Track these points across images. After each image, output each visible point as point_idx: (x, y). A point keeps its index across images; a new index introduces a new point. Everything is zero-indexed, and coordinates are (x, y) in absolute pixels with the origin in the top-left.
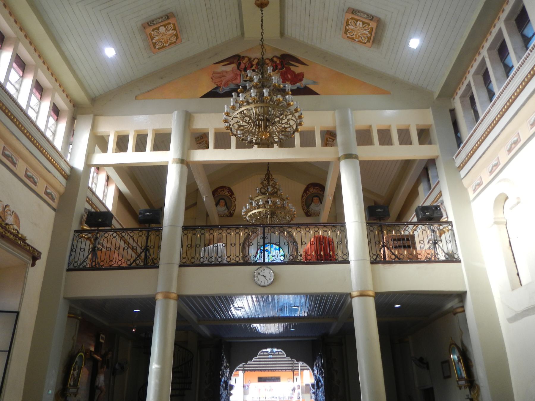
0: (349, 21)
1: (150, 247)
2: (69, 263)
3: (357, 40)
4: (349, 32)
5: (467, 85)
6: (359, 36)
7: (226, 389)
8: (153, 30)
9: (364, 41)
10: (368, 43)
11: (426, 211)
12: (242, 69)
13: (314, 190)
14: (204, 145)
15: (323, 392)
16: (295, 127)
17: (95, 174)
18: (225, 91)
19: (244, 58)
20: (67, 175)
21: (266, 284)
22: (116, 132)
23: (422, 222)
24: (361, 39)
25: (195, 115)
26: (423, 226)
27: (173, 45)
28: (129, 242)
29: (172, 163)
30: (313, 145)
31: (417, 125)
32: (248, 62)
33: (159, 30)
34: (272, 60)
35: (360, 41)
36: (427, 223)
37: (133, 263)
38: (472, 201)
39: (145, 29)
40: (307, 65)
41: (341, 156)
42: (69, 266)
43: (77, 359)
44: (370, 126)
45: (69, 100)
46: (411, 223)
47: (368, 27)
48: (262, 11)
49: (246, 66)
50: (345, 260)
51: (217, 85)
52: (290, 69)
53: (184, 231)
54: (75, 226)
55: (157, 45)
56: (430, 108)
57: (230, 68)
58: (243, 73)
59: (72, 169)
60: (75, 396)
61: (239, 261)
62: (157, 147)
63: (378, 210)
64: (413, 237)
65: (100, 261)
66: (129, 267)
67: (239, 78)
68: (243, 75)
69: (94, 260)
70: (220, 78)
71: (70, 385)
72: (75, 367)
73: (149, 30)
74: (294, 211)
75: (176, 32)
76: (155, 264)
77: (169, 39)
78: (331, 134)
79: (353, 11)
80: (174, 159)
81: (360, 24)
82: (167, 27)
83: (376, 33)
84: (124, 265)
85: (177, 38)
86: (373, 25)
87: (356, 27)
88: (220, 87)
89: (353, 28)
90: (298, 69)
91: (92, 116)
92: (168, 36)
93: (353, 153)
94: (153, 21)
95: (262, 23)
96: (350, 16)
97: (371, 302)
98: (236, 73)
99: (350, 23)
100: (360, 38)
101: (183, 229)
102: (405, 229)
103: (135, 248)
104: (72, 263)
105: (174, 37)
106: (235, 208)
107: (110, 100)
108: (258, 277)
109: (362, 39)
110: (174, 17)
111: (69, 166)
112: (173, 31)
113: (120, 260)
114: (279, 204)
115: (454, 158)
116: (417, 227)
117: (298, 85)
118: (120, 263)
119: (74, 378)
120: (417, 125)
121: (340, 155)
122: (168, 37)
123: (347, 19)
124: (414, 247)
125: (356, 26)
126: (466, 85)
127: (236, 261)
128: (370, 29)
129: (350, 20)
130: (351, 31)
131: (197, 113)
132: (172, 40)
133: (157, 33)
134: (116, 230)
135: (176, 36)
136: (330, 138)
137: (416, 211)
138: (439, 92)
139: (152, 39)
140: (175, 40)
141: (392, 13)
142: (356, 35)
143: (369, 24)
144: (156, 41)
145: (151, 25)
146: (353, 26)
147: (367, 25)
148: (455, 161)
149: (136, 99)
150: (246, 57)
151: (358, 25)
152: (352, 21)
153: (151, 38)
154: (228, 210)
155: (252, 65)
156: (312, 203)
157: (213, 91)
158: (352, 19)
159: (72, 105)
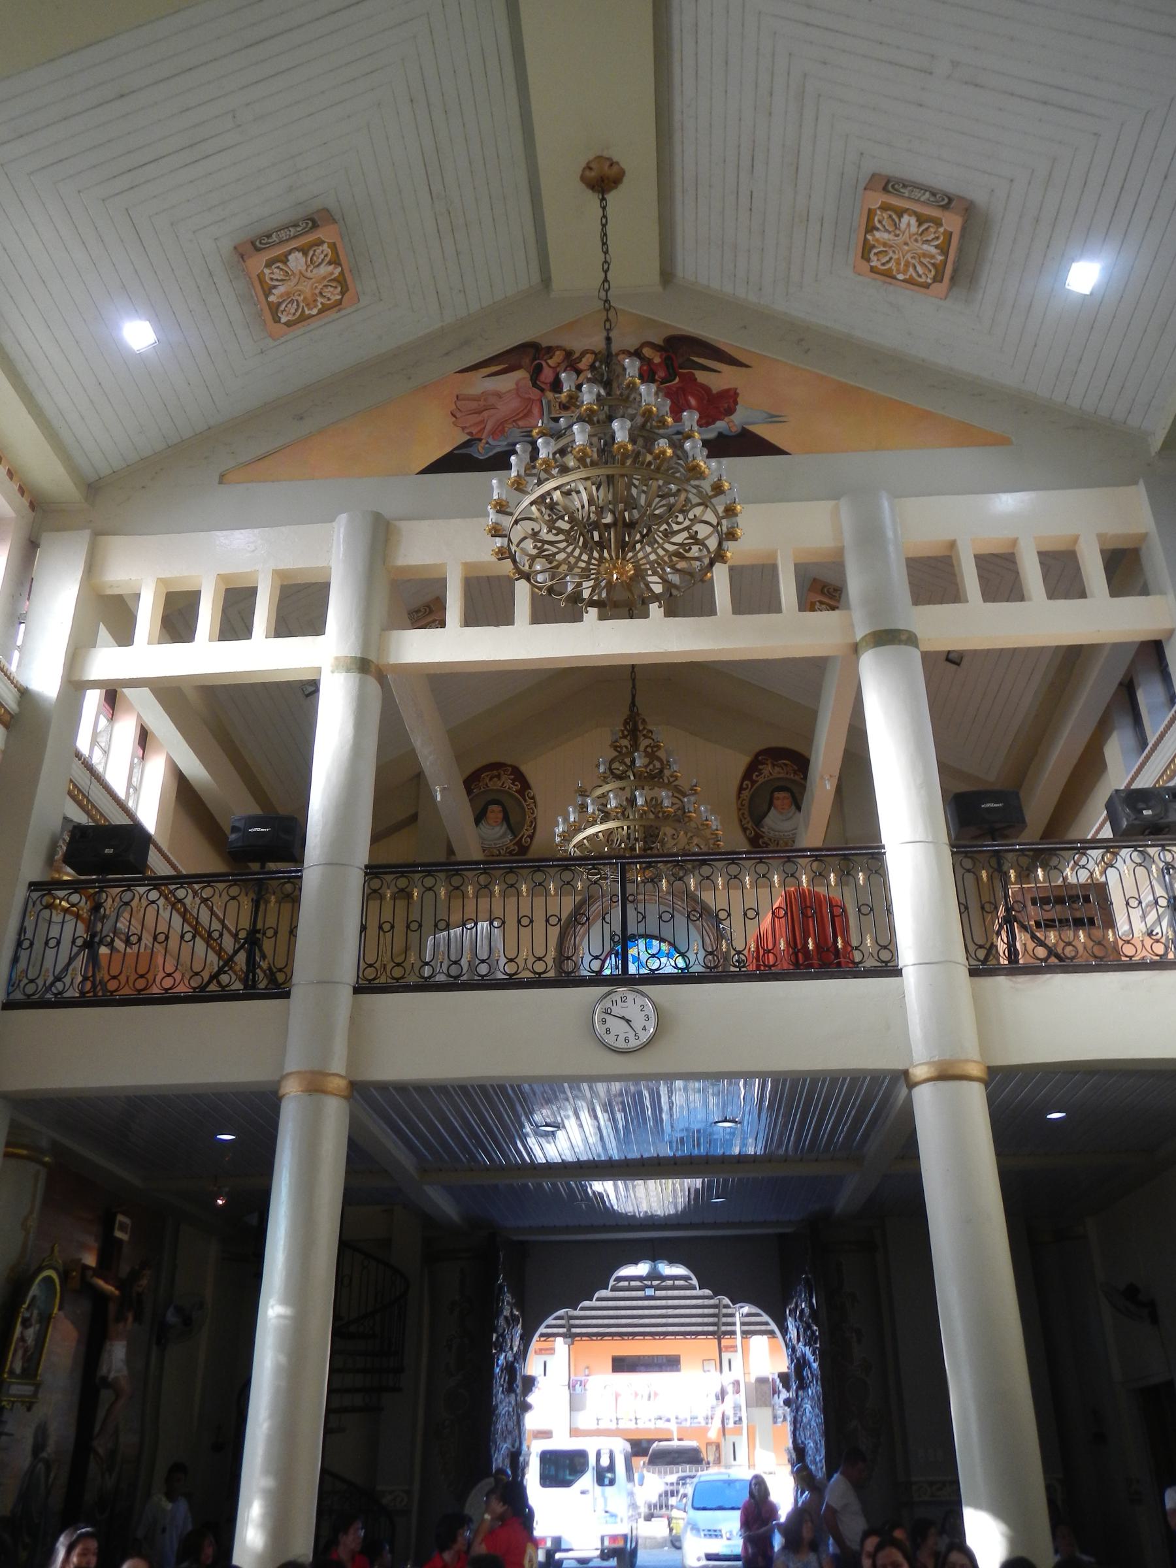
0: (875, 214)
1: (264, 934)
2: (12, 984)
3: (900, 277)
4: (875, 254)
6: (907, 264)
7: (510, 1389)
8: (269, 264)
9: (920, 280)
10: (936, 284)
11: (1141, 805)
13: (777, 769)
15: (819, 1399)
16: (712, 543)
17: (103, 722)
18: (495, 451)
19: (550, 350)
20: (10, 713)
21: (633, 1043)
22: (160, 581)
23: (1134, 838)
24: (914, 275)
25: (404, 526)
26: (1136, 853)
27: (332, 315)
28: (197, 919)
29: (333, 672)
30: (773, 606)
31: (1101, 537)
32: (563, 361)
33: (288, 263)
35: (910, 281)
36: (1150, 843)
37: (209, 982)
39: (244, 261)
40: (747, 366)
41: (863, 639)
42: (8, 994)
43: (34, 1290)
44: (953, 545)
45: (17, 488)
46: (1095, 843)
47: (935, 233)
48: (603, 199)
50: (886, 966)
51: (470, 434)
52: (696, 379)
53: (371, 879)
54: (32, 868)
55: (282, 312)
56: (1141, 482)
57: (507, 383)
58: (550, 395)
59: (24, 693)
60: (29, 1409)
61: (544, 972)
62: (284, 627)
63: (988, 805)
64: (1101, 890)
65: (107, 978)
66: (200, 996)
67: (536, 410)
68: (549, 402)
69: (90, 974)
71: (12, 1373)
72: (27, 1315)
73: (257, 263)
74: (714, 827)
75: (339, 269)
76: (278, 986)
77: (321, 293)
79: (889, 185)
80: (337, 658)
81: (909, 225)
82: (311, 253)
83: (960, 250)
84: (182, 989)
85: (344, 289)
86: (952, 222)
87: (897, 236)
88: (480, 440)
89: (889, 240)
90: (718, 379)
91: (86, 534)
93: (901, 628)
94: (269, 236)
95: (605, 235)
96: (877, 199)
97: (975, 1097)
98: (527, 396)
99: (880, 222)
100: (911, 270)
101: (366, 874)
102: (1076, 863)
103: (216, 935)
104: (19, 985)
105: (336, 287)
106: (535, 828)
107: (143, 487)
108: (604, 1021)
109: (917, 272)
110: (335, 221)
111: (15, 687)
112: (331, 268)
113: (169, 975)
114: (668, 807)
116: (1115, 854)
117: (720, 425)
118: (168, 983)
119: (26, 1351)
120: (1101, 537)
121: (859, 636)
122: (316, 287)
124: (1110, 923)
125: (898, 232)
127: (535, 973)
128: (942, 238)
129: (878, 212)
130: (882, 249)
131: (409, 519)
132: (329, 295)
133: (282, 273)
134: (158, 882)
137: (1109, 806)
138: (1166, 431)
139: (266, 288)
140: (339, 297)
141: (1012, 181)
142: (898, 263)
143: (938, 223)
145: (264, 246)
146: (889, 232)
147: (932, 225)
149: (221, 482)
150: (559, 348)
151: (903, 225)
152: (885, 215)
154: (515, 835)
156: (769, 809)
158: (885, 207)
159: (27, 504)
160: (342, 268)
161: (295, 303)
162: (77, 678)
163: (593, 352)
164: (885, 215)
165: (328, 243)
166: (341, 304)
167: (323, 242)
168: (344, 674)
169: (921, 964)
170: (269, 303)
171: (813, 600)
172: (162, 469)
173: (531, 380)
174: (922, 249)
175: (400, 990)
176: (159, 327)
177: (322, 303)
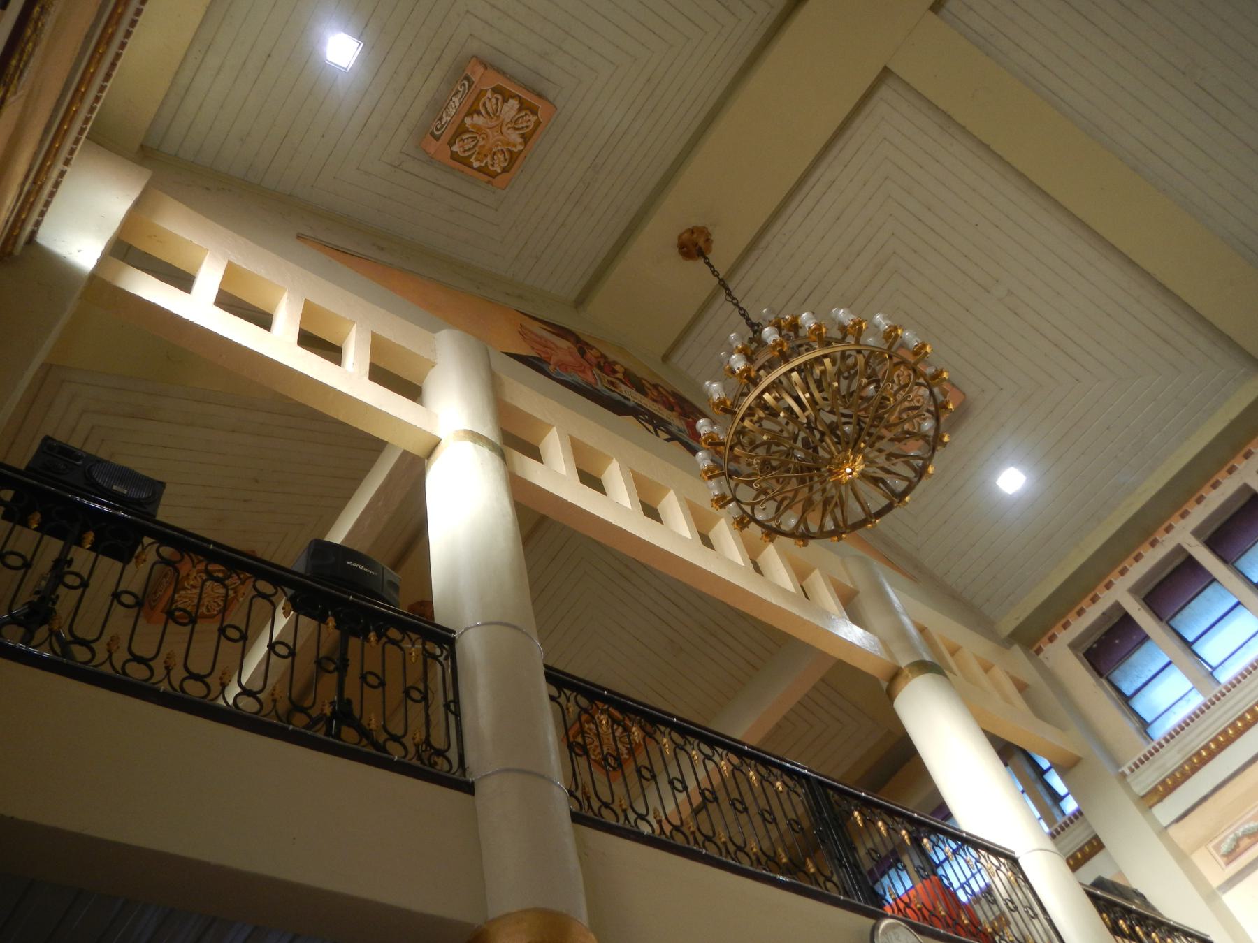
5: (1104, 614)
8: (496, 90)
31: (1007, 673)
33: (505, 104)
34: (656, 387)
38: (1220, 888)
51: (538, 354)
57: (564, 344)
58: (599, 372)
68: (598, 374)
70: (545, 347)
75: (521, 148)
77: (494, 153)
82: (523, 114)
92: (500, 143)
99: (898, 376)
112: (520, 140)
115: (1127, 772)
122: (497, 146)
132: (496, 162)
133: (494, 107)
135: (513, 157)
138: (1017, 623)
140: (499, 171)
144: (470, 129)
148: (1129, 780)
153: (472, 106)
157: (529, 359)
160: (523, 150)
161: (474, 143)
164: (906, 373)
166: (494, 177)
168: (488, 450)
172: (229, 191)
176: (363, 59)
177: (487, 163)
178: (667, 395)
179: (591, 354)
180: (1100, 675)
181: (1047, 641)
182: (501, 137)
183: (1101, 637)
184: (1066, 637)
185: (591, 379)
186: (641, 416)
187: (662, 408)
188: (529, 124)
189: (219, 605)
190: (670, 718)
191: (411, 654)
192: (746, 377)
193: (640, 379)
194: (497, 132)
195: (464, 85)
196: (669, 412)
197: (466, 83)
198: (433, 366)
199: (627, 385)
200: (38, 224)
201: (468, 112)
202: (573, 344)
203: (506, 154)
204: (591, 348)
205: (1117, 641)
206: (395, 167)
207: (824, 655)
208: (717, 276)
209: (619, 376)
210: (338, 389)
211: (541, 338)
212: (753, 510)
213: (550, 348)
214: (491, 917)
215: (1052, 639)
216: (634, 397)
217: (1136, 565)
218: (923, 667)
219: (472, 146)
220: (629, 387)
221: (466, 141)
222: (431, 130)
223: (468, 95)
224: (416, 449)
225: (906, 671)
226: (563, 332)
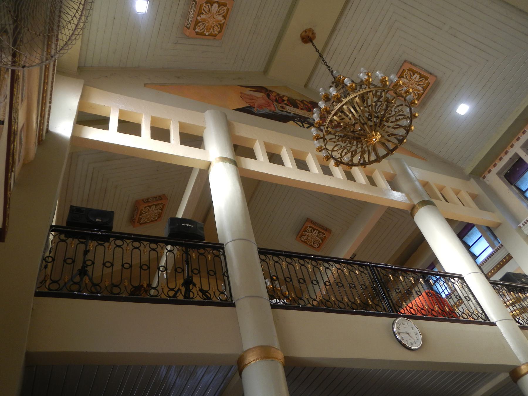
0: (405, 72)
5: (510, 159)
12: (273, 100)
14: (158, 211)
19: (272, 92)
31: (467, 192)
33: (212, 6)
34: (302, 102)
41: (417, 203)
47: (424, 82)
49: (276, 98)
57: (260, 95)
58: (276, 103)
68: (276, 105)
75: (223, 21)
77: (213, 27)
78: (312, 222)
81: (416, 78)
87: (410, 81)
88: (255, 108)
92: (214, 22)
99: (405, 75)
112: (222, 18)
115: (522, 226)
122: (214, 24)
123: (404, 69)
125: (410, 80)
126: (509, 158)
128: (425, 85)
132: (215, 30)
133: (208, 9)
135: (221, 26)
136: (310, 227)
138: (472, 168)
139: (200, 12)
140: (217, 33)
143: (427, 79)
144: (201, 21)
147: (424, 79)
150: (274, 92)
151: (413, 78)
155: (284, 101)
161: (204, 26)
162: (77, 135)
163: (287, 97)
164: (408, 73)
165: (228, 7)
167: (226, 6)
168: (229, 164)
169: (500, 320)
170: (197, 19)
171: (307, 226)
173: (267, 97)
174: (417, 88)
175: (295, 309)
177: (211, 32)
178: (308, 104)
179: (273, 96)
180: (512, 184)
181: (488, 173)
182: (214, 20)
183: (511, 168)
184: (495, 170)
185: (273, 108)
186: (296, 120)
187: (305, 111)
188: (224, 11)
189: (157, 216)
190: (310, 256)
191: (209, 257)
192: (325, 111)
193: (295, 100)
194: (212, 18)
195: (194, 4)
196: (309, 113)
197: (194, 2)
198: (205, 128)
199: (289, 106)
200: (48, 125)
201: (198, 14)
202: (264, 93)
203: (218, 25)
204: (272, 92)
205: (518, 169)
206: (175, 43)
207: (382, 206)
208: (318, 52)
209: (286, 102)
210: (169, 153)
211: (250, 96)
212: (341, 159)
213: (255, 100)
214: (244, 350)
215: (489, 172)
216: (292, 110)
217: (506, 156)
218: (424, 203)
219: (203, 27)
220: (291, 106)
221: (200, 26)
222: (185, 25)
223: (196, 8)
224: (203, 167)
225: (417, 206)
226: (259, 89)
